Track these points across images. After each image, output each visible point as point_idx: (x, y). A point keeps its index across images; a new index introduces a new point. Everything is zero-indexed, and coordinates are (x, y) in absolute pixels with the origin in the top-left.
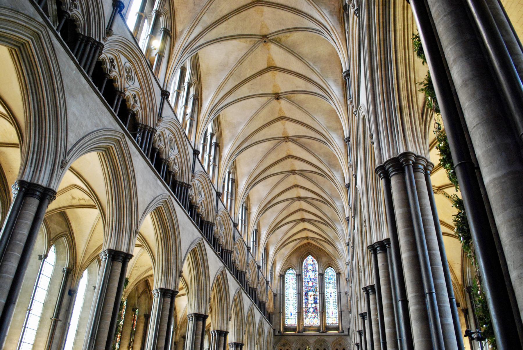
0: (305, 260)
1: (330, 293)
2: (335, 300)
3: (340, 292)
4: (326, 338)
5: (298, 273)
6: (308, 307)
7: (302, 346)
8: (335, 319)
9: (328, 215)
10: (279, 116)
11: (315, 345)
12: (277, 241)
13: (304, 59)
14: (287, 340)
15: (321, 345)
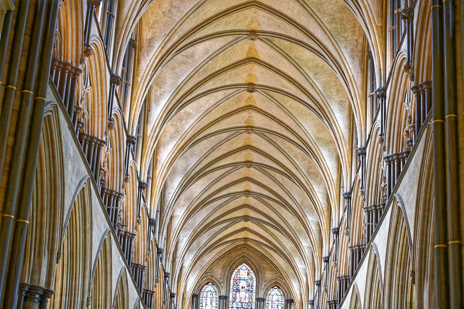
0: (236, 271)
5: (223, 293)
9: (289, 222)
10: (246, 105)
12: (199, 245)
13: (301, 68)
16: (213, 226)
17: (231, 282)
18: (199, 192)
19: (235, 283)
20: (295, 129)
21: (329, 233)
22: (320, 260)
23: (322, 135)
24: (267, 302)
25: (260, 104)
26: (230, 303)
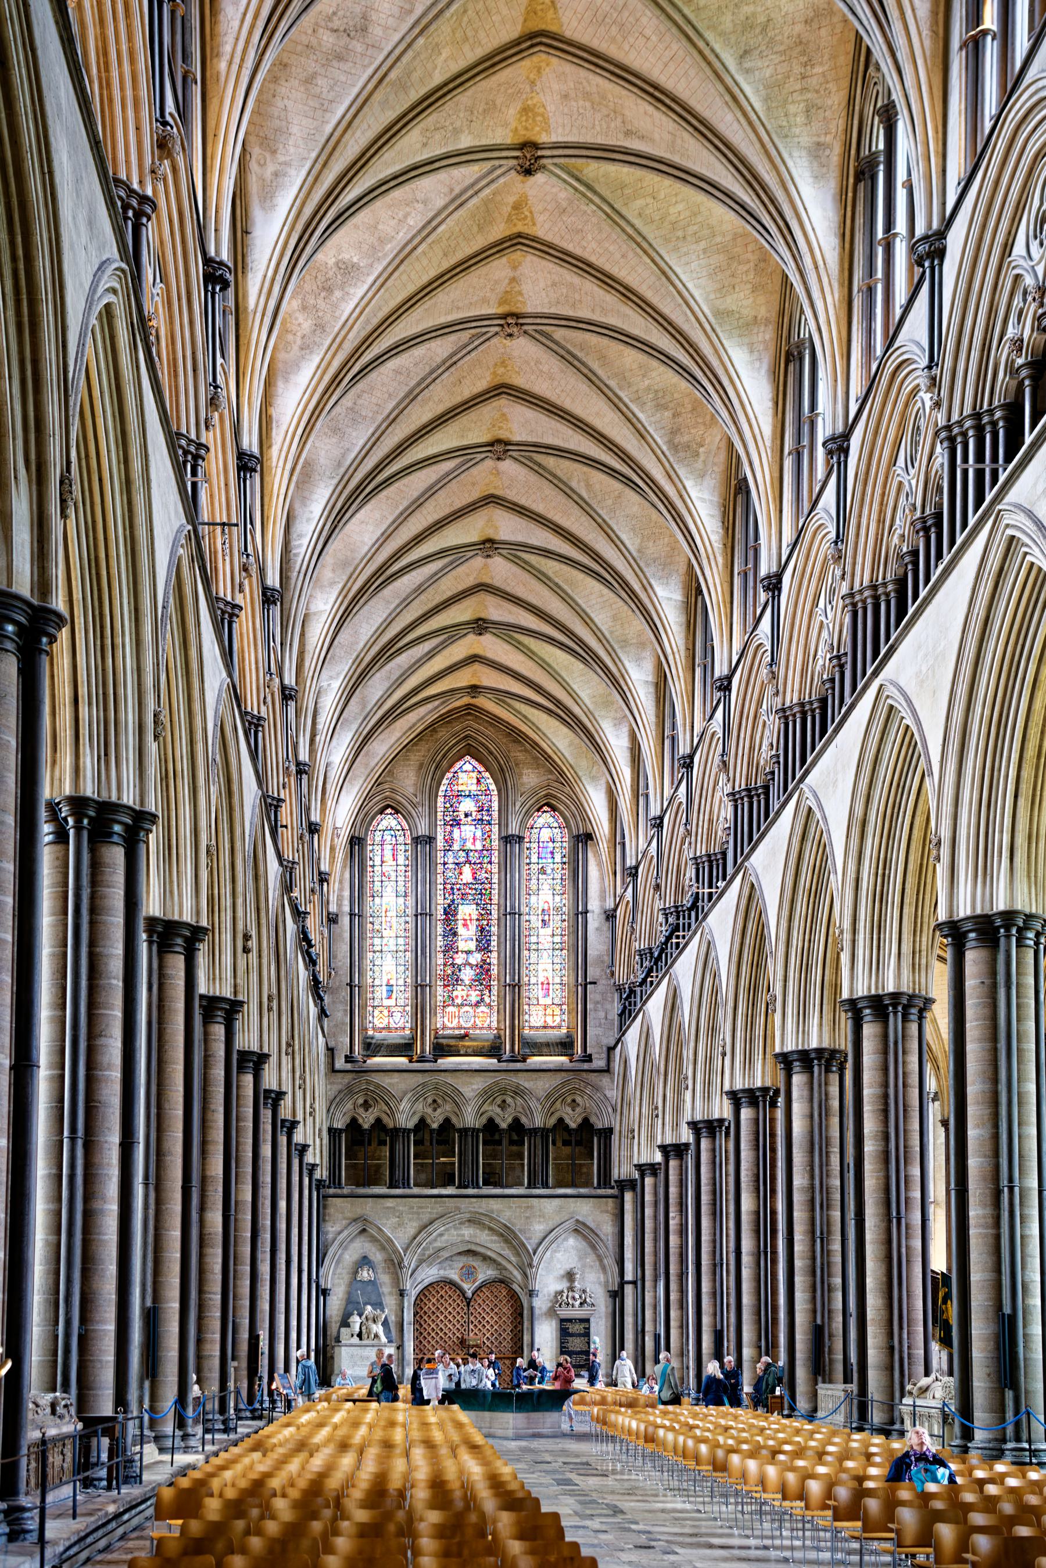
1: (543, 910)
2: (557, 939)
3: (586, 912)
4: (525, 1082)
5: (423, 829)
6: (453, 965)
7: (435, 1110)
8: (557, 1011)
11: (484, 1102)
12: (364, 707)
14: (378, 1086)
15: (503, 1105)
16: (400, 651)
17: (439, 805)
18: (370, 543)
19: (448, 805)
20: (649, 295)
21: (729, 610)
22: (688, 702)
23: (730, 302)
24: (528, 845)
25: (547, 226)
26: (440, 854)
